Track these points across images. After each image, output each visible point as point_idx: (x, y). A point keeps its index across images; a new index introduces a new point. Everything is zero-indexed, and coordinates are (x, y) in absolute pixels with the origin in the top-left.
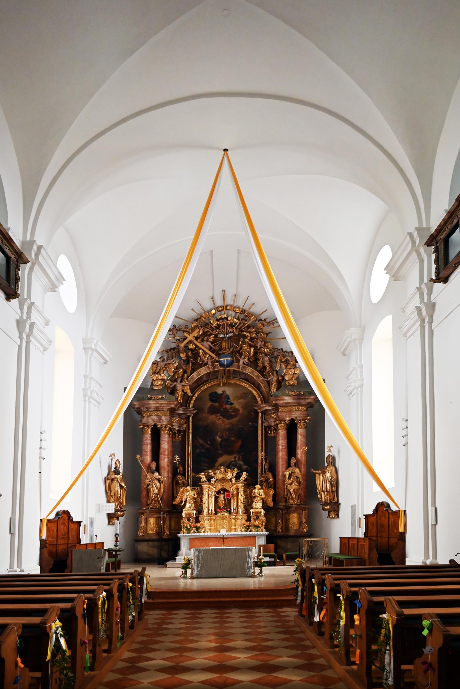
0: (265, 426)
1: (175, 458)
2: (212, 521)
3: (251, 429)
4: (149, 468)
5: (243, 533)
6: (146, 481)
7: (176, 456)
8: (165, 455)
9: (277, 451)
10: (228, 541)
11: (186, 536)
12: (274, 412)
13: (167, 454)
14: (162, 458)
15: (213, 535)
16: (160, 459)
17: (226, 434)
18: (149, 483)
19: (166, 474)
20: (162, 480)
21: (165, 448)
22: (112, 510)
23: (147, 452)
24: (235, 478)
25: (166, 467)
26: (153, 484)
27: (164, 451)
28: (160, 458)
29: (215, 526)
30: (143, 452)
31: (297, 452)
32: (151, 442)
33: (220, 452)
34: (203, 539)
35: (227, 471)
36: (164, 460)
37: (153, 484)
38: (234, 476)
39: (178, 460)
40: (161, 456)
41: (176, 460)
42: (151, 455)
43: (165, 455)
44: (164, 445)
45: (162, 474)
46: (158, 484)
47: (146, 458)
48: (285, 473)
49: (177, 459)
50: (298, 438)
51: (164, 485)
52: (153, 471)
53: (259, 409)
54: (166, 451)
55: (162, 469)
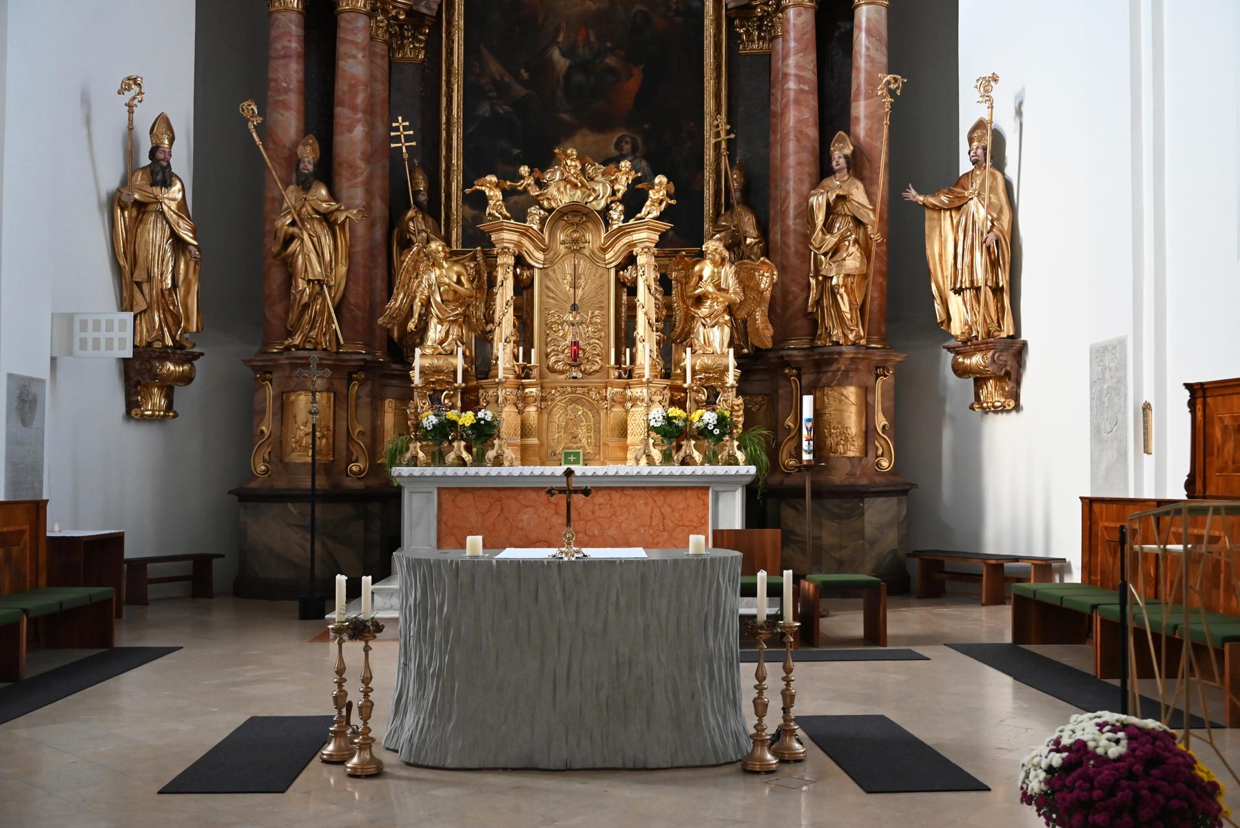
0: (730, 6)
1: (397, 129)
2: (532, 410)
3: (677, 19)
4: (294, 162)
5: (656, 470)
6: (279, 224)
7: (400, 118)
9: (775, 115)
10: (594, 505)
11: (422, 477)
13: (362, 102)
15: (532, 476)
16: (337, 129)
17: (587, 42)
18: (291, 229)
19: (353, 192)
21: (353, 77)
22: (122, 341)
24: (621, 208)
25: (361, 164)
26: (306, 237)
27: (352, 87)
28: (336, 120)
30: (270, 93)
31: (853, 113)
33: (566, 117)
34: (495, 493)
35: (590, 170)
36: (350, 130)
37: (306, 237)
38: (620, 195)
39: (408, 139)
40: (338, 110)
41: (397, 139)
42: (302, 108)
43: (354, 109)
44: (351, 61)
45: (344, 194)
46: (327, 241)
47: (281, 118)
48: (813, 200)
49: (403, 134)
50: (855, 48)
51: (351, 246)
54: (361, 88)
55: (345, 173)
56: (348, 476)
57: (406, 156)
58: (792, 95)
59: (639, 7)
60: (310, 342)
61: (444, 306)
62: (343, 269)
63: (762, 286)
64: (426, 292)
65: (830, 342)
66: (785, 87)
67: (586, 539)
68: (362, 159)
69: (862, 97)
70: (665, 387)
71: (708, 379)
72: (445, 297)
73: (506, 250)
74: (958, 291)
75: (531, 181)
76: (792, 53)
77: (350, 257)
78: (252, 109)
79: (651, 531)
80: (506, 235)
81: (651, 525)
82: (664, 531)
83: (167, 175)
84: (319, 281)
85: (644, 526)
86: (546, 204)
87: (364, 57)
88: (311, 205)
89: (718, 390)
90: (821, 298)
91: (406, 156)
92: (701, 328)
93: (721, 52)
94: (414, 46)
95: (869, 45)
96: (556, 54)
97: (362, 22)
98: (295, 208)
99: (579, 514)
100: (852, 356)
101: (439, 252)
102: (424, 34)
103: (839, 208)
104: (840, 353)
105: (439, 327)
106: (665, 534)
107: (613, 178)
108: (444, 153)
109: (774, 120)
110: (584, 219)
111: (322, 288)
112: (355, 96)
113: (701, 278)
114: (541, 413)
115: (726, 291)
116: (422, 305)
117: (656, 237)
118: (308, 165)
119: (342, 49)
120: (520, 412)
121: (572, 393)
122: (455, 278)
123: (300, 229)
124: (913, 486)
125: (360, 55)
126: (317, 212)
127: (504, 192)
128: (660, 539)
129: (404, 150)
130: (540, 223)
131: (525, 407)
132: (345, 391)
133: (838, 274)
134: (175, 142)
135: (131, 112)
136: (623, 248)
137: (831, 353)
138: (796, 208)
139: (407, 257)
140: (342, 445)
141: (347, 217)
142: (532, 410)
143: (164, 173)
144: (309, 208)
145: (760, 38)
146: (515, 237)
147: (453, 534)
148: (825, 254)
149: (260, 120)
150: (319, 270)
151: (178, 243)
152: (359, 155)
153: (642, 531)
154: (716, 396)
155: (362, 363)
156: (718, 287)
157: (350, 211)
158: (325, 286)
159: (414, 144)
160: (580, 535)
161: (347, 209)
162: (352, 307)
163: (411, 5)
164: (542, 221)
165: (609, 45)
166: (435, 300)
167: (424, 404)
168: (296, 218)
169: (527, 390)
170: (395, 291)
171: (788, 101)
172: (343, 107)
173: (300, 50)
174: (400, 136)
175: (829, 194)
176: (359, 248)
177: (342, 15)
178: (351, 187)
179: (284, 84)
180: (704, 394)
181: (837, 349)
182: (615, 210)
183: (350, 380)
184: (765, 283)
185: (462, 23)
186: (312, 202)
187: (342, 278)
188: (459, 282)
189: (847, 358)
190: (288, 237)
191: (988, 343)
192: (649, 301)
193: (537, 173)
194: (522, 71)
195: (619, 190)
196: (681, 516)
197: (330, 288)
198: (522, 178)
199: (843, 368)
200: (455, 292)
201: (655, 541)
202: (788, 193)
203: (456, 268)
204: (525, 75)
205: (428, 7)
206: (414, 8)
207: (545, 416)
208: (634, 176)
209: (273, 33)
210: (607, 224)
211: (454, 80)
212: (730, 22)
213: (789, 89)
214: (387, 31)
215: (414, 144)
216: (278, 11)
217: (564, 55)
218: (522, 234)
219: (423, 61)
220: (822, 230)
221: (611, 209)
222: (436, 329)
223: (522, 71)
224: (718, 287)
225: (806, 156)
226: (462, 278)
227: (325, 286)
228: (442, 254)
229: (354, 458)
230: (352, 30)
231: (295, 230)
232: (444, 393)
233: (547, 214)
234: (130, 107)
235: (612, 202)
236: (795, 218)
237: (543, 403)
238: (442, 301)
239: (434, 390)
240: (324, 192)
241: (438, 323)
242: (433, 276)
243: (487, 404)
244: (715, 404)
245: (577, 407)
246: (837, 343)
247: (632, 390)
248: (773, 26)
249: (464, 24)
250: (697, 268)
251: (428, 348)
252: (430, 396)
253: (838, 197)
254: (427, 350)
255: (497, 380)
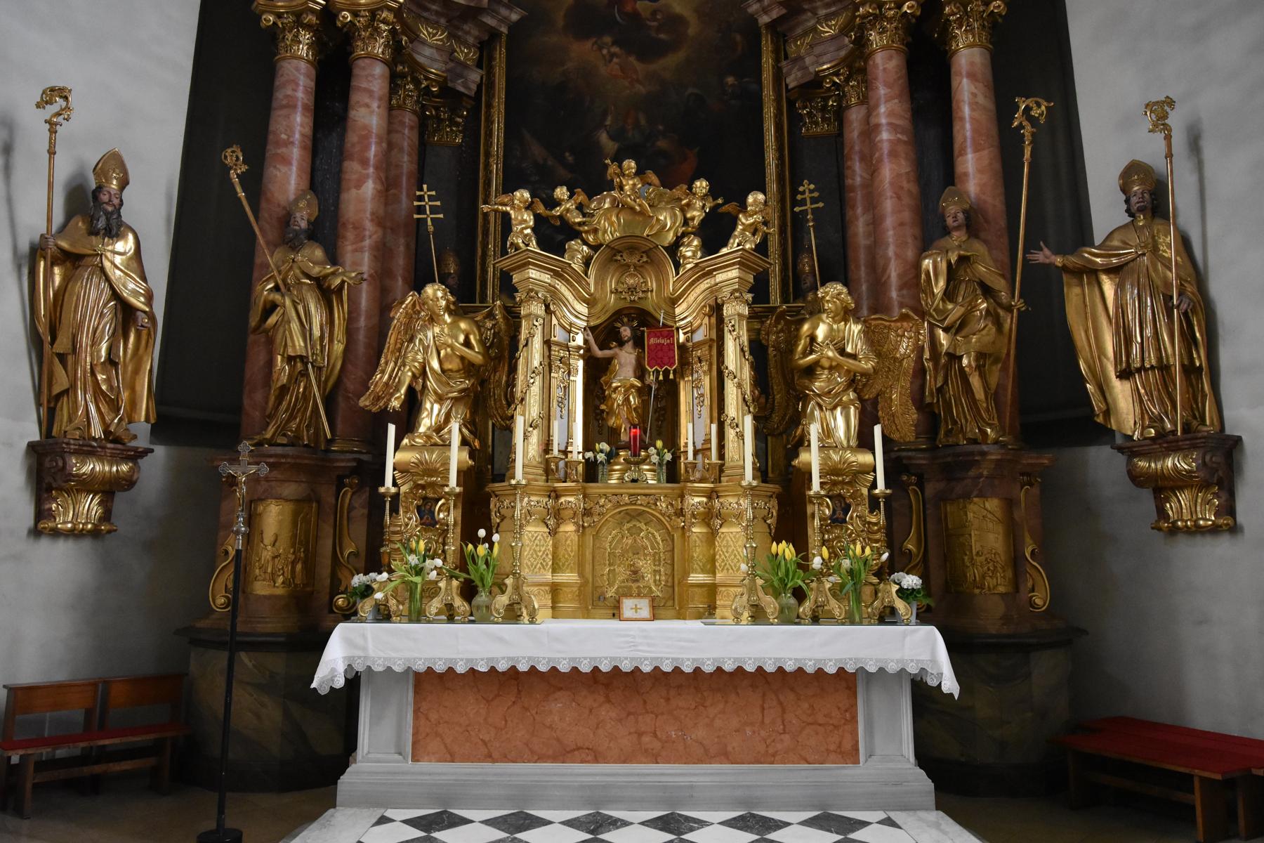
8: (364, 162)
12: (827, 15)
13: (375, 156)
14: (354, 177)
20: (338, 281)
21: (366, 127)
23: (289, 143)
27: (365, 139)
29: (588, 568)
32: (310, 101)
36: (360, 183)
37: (288, 302)
52: (297, 234)
53: (765, 11)
54: (373, 140)
56: (332, 611)
57: (431, 228)
58: (886, 148)
59: (690, 90)
60: (284, 435)
61: (444, 379)
62: (339, 348)
63: (902, 351)
64: (420, 357)
65: (965, 438)
66: (878, 139)
67: (657, 745)
68: (372, 220)
69: (969, 150)
70: (771, 496)
71: (834, 483)
72: (447, 366)
73: (532, 294)
74: (1125, 374)
75: (570, 205)
76: (883, 99)
77: (350, 333)
78: (238, 158)
79: (763, 733)
80: (533, 273)
81: (763, 722)
82: (784, 732)
83: (114, 222)
84: (301, 357)
85: (752, 724)
86: (591, 238)
87: (379, 107)
88: (300, 268)
89: (849, 501)
90: (946, 382)
91: (431, 228)
92: (817, 413)
93: (783, 133)
94: (451, 130)
95: (975, 91)
96: (604, 137)
97: (379, 70)
98: (280, 272)
99: (645, 702)
100: (999, 457)
101: (437, 298)
102: (461, 116)
103: (961, 272)
104: (983, 454)
105: (436, 407)
106: (786, 737)
107: (684, 202)
108: (480, 238)
109: (852, 194)
110: (645, 259)
111: (307, 369)
112: (367, 148)
113: (813, 338)
114: (583, 533)
115: (854, 356)
116: (414, 376)
117: (751, 278)
118: (302, 220)
119: (355, 97)
120: (553, 532)
121: (631, 504)
122: (462, 338)
123: (283, 296)
124: (1084, 632)
125: (375, 105)
126: (308, 276)
127: (537, 217)
128: (779, 746)
129: (429, 222)
130: (583, 263)
131: (558, 525)
132: (333, 501)
133: (968, 354)
134: (127, 187)
135: (53, 131)
136: (701, 297)
137: (972, 454)
138: (900, 276)
139: (398, 311)
140: (324, 571)
141: (343, 282)
142: (569, 528)
143: (108, 219)
144: (298, 271)
145: (824, 119)
146: (546, 278)
147: (437, 734)
148: (946, 330)
149: (244, 168)
150: (302, 344)
151: (126, 313)
152: (368, 215)
153: (749, 733)
154: (846, 509)
155: (354, 464)
156: (842, 351)
157: (347, 274)
158: (310, 366)
159: (441, 216)
160: (646, 739)
161: (343, 274)
162: (350, 395)
163: (446, 78)
164: (587, 262)
165: (661, 127)
166: (432, 369)
167: (410, 519)
168: (280, 282)
169: (562, 500)
170: (383, 360)
171: (882, 155)
172: (353, 161)
173: (306, 101)
174: (425, 206)
175: (950, 254)
176: (362, 322)
177: (356, 62)
178: (356, 250)
179: (284, 136)
180: (828, 506)
181: (976, 448)
182: (689, 245)
183: (340, 485)
184: (905, 347)
185: (502, 107)
186: (301, 264)
187: (337, 358)
188: (467, 343)
189: (991, 460)
190: (268, 306)
191: (1197, 438)
192: (741, 368)
193: (581, 197)
194: (567, 154)
195: (693, 219)
196: (812, 707)
197: (319, 369)
198: (557, 203)
199: (985, 473)
200: (462, 358)
201: (771, 751)
202: (888, 260)
203: (463, 325)
204: (569, 158)
205: (465, 85)
206: (450, 84)
207: (589, 540)
208: (712, 205)
209: (277, 83)
210: (677, 266)
211: (492, 160)
212: (791, 104)
213: (881, 141)
214: (417, 102)
215: (441, 216)
216: (284, 59)
217: (612, 138)
218: (557, 275)
219: (460, 146)
220: (942, 299)
221: (683, 244)
222: (432, 409)
223: (567, 154)
224: (842, 351)
225: (907, 215)
226: (472, 337)
227: (310, 366)
228: (444, 303)
229: (342, 588)
230: (367, 76)
231: (277, 297)
232: (440, 503)
233: (592, 253)
234: (52, 126)
235: (684, 235)
236: (901, 288)
237: (586, 519)
238: (443, 371)
239: (425, 498)
240: (319, 253)
241: (436, 401)
242: (430, 334)
243: (502, 520)
244: (845, 521)
245: (638, 524)
246: (974, 441)
247: (721, 500)
248: (845, 95)
249: (505, 108)
250: (806, 327)
251: (418, 437)
252: (418, 508)
253: (962, 259)
254: (417, 440)
255: (513, 482)
